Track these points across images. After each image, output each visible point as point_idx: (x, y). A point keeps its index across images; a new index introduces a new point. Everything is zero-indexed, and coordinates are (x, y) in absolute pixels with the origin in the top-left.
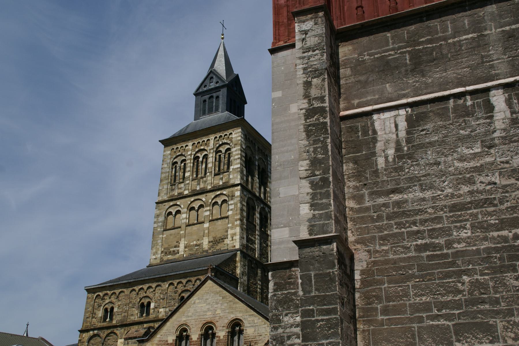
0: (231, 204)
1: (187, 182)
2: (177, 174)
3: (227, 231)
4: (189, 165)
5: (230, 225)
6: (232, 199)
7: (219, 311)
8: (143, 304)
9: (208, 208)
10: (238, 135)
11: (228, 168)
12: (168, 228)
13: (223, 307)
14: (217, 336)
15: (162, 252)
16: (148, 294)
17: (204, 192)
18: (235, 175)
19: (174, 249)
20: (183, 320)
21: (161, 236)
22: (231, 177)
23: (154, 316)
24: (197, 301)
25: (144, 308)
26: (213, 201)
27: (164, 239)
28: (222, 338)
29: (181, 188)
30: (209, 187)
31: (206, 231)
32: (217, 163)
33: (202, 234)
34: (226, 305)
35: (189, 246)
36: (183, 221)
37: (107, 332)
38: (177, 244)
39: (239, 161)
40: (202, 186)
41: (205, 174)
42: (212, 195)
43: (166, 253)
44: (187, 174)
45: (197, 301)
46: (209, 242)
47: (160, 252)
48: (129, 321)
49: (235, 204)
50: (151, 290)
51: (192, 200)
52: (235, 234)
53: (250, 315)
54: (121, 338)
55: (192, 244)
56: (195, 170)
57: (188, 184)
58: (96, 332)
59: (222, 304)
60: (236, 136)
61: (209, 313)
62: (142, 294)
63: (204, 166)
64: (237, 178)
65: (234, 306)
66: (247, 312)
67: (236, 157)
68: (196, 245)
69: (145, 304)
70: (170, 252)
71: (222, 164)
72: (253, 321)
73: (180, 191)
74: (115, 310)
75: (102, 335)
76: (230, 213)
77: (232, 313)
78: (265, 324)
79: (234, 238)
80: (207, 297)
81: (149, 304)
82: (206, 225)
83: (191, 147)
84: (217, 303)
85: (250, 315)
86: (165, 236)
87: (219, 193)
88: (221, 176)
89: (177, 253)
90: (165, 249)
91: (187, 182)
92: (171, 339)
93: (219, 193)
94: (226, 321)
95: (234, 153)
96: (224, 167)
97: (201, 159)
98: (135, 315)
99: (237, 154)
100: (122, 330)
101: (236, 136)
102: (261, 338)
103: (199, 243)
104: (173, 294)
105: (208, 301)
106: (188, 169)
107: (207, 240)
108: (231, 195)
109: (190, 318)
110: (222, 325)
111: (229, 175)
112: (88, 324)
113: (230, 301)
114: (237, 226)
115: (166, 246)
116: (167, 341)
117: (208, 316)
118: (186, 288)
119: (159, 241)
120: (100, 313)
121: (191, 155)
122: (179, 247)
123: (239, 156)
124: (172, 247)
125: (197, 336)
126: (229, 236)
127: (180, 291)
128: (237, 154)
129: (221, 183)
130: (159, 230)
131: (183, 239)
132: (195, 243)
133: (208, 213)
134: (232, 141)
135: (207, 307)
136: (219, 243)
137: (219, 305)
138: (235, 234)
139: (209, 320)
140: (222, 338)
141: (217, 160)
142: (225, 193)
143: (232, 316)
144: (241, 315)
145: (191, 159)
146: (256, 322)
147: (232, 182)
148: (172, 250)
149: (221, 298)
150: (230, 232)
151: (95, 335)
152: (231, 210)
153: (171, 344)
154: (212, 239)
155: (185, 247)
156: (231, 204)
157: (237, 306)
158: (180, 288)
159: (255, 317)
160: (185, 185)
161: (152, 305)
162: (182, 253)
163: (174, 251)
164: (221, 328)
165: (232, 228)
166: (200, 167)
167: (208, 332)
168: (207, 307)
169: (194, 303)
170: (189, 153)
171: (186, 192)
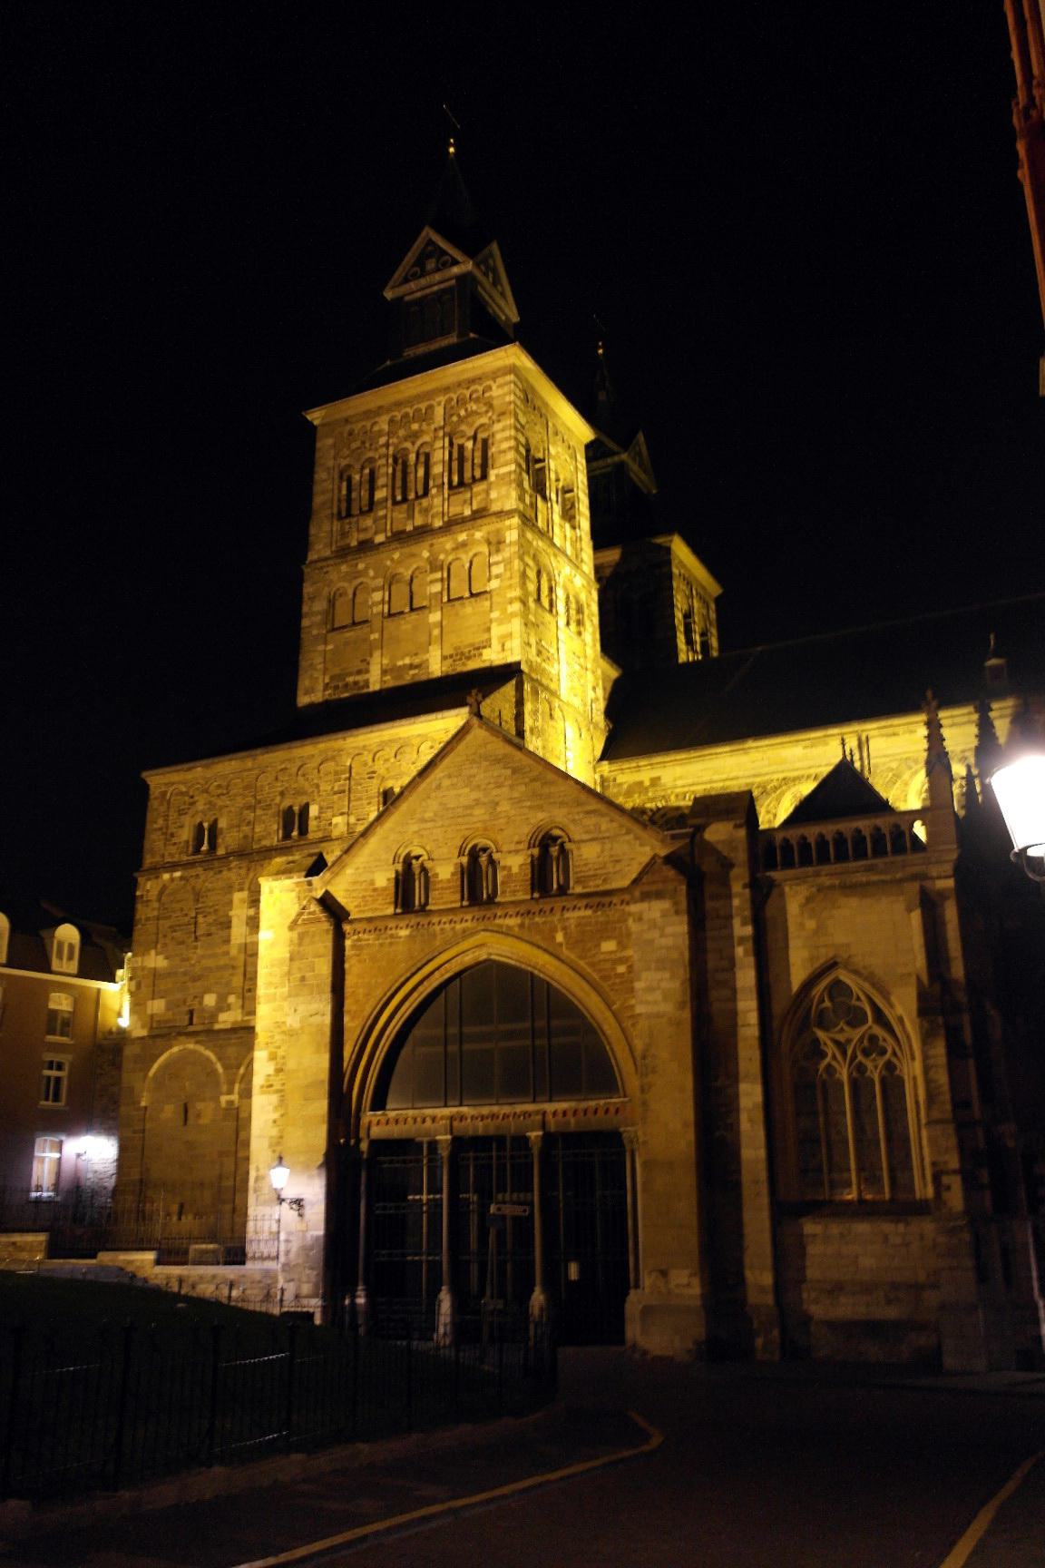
1: (381, 513)
2: (354, 495)
3: (489, 630)
4: (383, 470)
5: (495, 615)
6: (498, 551)
7: (505, 807)
9: (438, 575)
10: (506, 389)
11: (484, 477)
13: (516, 794)
14: (504, 868)
18: (504, 490)
21: (321, 648)
22: (493, 495)
24: (446, 783)
27: (329, 656)
28: (515, 870)
29: (366, 530)
31: (436, 632)
32: (455, 465)
33: (424, 638)
34: (523, 788)
36: (375, 610)
38: (363, 666)
39: (511, 455)
40: (419, 521)
44: (380, 494)
45: (446, 783)
46: (444, 658)
47: (321, 687)
49: (508, 562)
52: (510, 635)
53: (588, 812)
54: (241, 890)
55: (400, 663)
56: (399, 483)
57: (385, 517)
58: (178, 874)
59: (511, 787)
60: (500, 392)
61: (478, 811)
63: (421, 472)
64: (508, 496)
65: (546, 790)
66: (579, 804)
67: (505, 446)
68: (412, 666)
69: (296, 809)
70: (346, 685)
71: (468, 466)
72: (597, 826)
73: (363, 536)
74: (222, 824)
76: (494, 584)
77: (541, 808)
78: (628, 832)
79: (508, 645)
80: (474, 771)
81: (305, 809)
82: (435, 617)
83: (386, 427)
84: (499, 786)
85: (588, 812)
86: (330, 647)
90: (332, 678)
91: (381, 513)
94: (525, 831)
95: (498, 436)
97: (412, 457)
99: (507, 439)
101: (500, 392)
102: (618, 867)
103: (417, 661)
105: (475, 782)
106: (381, 481)
107: (438, 653)
108: (494, 540)
109: (429, 825)
110: (516, 838)
111: (488, 493)
112: (158, 859)
113: (534, 780)
114: (513, 615)
115: (337, 671)
116: (372, 882)
119: (318, 660)
120: (186, 835)
121: (387, 445)
122: (367, 671)
123: (512, 443)
124: (351, 674)
125: (451, 869)
126: (495, 642)
128: (507, 439)
130: (315, 632)
131: (377, 654)
132: (407, 661)
133: (437, 588)
135: (475, 795)
137: (505, 790)
138: (510, 635)
140: (515, 870)
141: (455, 455)
143: (540, 817)
144: (564, 811)
145: (387, 456)
146: (604, 827)
148: (351, 679)
149: (509, 772)
150: (496, 631)
152: (497, 576)
153: (384, 889)
154: (448, 652)
156: (497, 563)
157: (553, 789)
159: (603, 815)
160: (375, 521)
161: (314, 811)
164: (513, 847)
165: (500, 622)
166: (411, 477)
168: (475, 795)
169: (439, 787)
170: (383, 440)
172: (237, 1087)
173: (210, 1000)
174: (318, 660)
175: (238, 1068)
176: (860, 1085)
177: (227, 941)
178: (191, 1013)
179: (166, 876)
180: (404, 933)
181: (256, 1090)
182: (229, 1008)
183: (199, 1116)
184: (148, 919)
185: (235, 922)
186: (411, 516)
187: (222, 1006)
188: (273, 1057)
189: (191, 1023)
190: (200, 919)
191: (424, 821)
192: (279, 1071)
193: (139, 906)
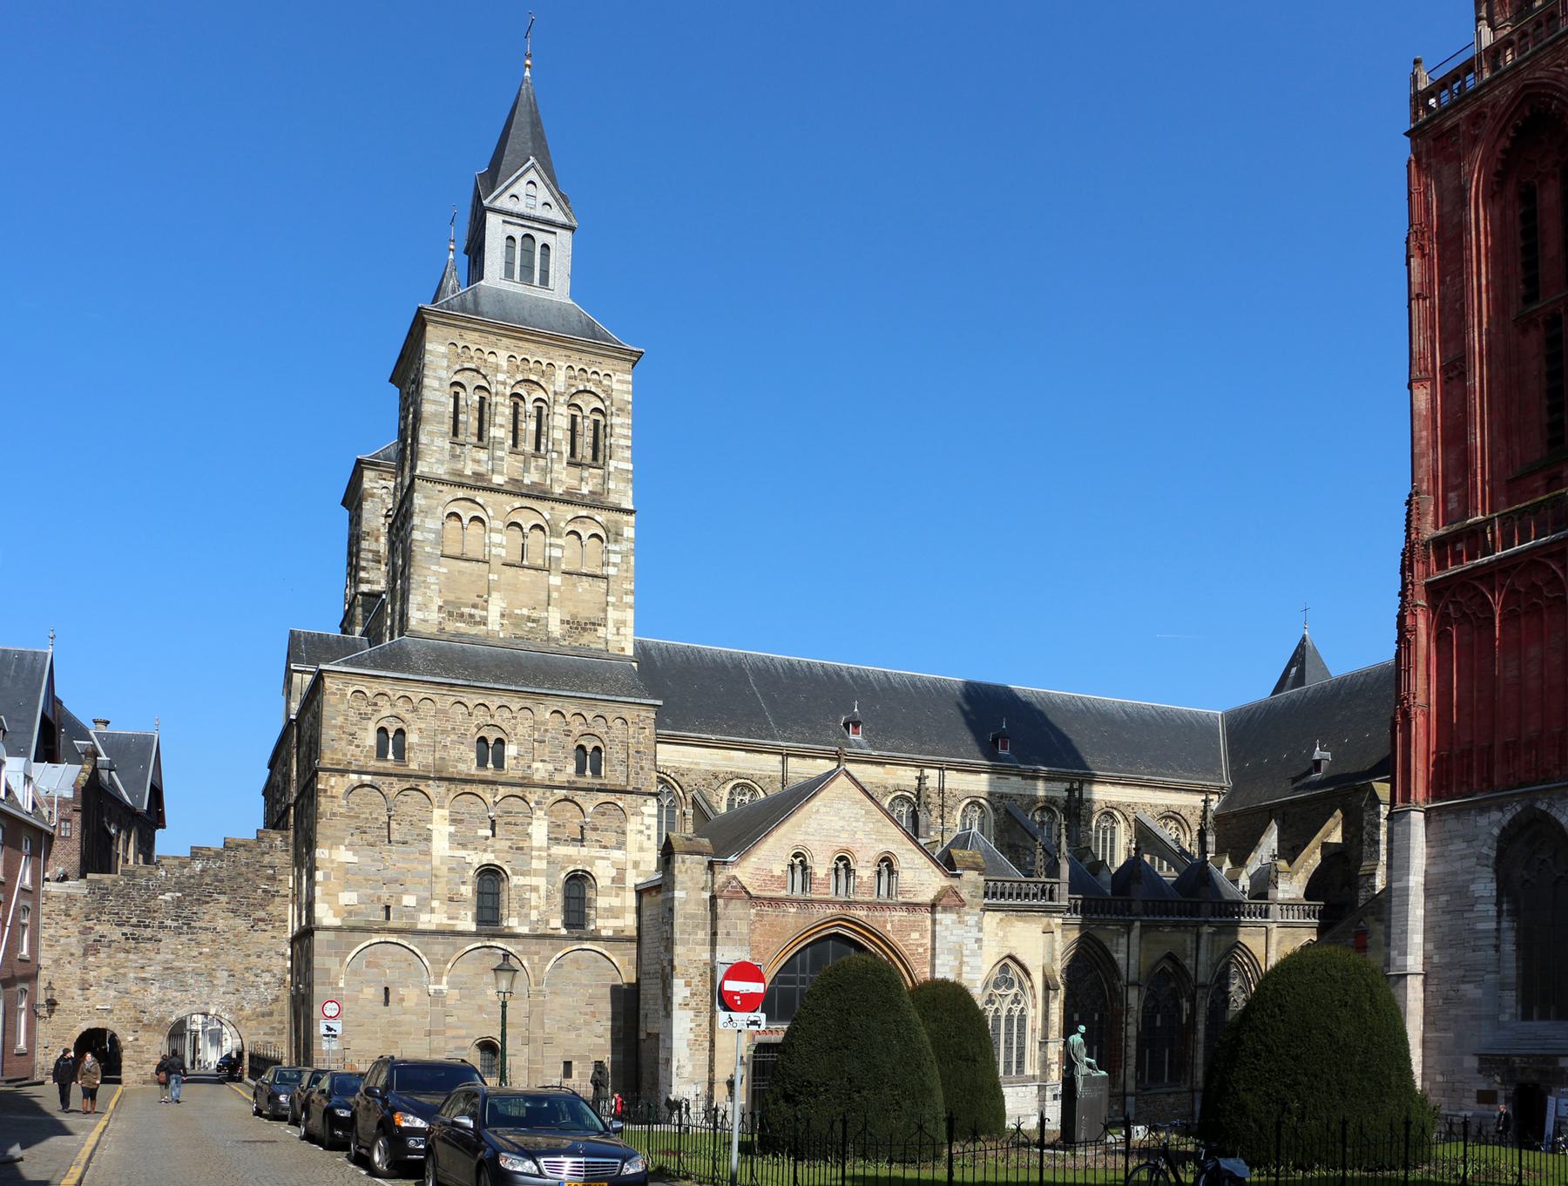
0: (615, 552)
6: (616, 541)
7: (860, 835)
8: (483, 740)
12: (447, 552)
15: (440, 608)
16: (497, 721)
17: (543, 495)
19: (473, 611)
20: (799, 838)
21: (434, 568)
22: (612, 485)
23: (519, 774)
24: (823, 810)
25: (490, 750)
26: (569, 528)
30: (558, 490)
35: (510, 616)
37: (398, 785)
41: (538, 448)
42: (570, 512)
43: (450, 614)
45: (823, 810)
46: (562, 622)
48: (451, 771)
50: (507, 714)
51: (517, 505)
54: (442, 807)
58: (367, 779)
61: (844, 835)
62: (480, 717)
67: (623, 442)
68: (529, 619)
69: (491, 743)
70: (462, 615)
74: (412, 738)
75: (385, 789)
82: (555, 580)
87: (584, 512)
88: (585, 474)
89: (477, 623)
92: (780, 868)
93: (584, 512)
96: (585, 451)
98: (469, 766)
99: (625, 437)
100: (443, 790)
103: (535, 615)
104: (562, 737)
115: (451, 597)
117: (843, 841)
118: (591, 731)
120: (371, 739)
124: (466, 605)
127: (577, 732)
128: (625, 437)
129: (585, 491)
132: (525, 612)
134: (609, 396)
136: (584, 629)
139: (844, 846)
142: (597, 518)
147: (613, 499)
148: (466, 610)
151: (362, 786)
155: (503, 616)
156: (615, 552)
158: (577, 727)
161: (511, 750)
162: (497, 628)
163: (471, 616)
167: (844, 864)
168: (841, 823)
171: (498, 479)
172: (445, 979)
173: (409, 900)
174: (431, 579)
175: (446, 963)
176: (1009, 1019)
177: (428, 853)
178: (388, 908)
179: (354, 777)
180: (793, 910)
181: (675, 1006)
182: (432, 911)
183: (402, 1000)
184: (334, 814)
185: (435, 835)
186: (526, 469)
187: (424, 905)
188: (688, 984)
189: (388, 918)
190: (393, 825)
191: (807, 833)
192: (693, 995)
193: (322, 800)
